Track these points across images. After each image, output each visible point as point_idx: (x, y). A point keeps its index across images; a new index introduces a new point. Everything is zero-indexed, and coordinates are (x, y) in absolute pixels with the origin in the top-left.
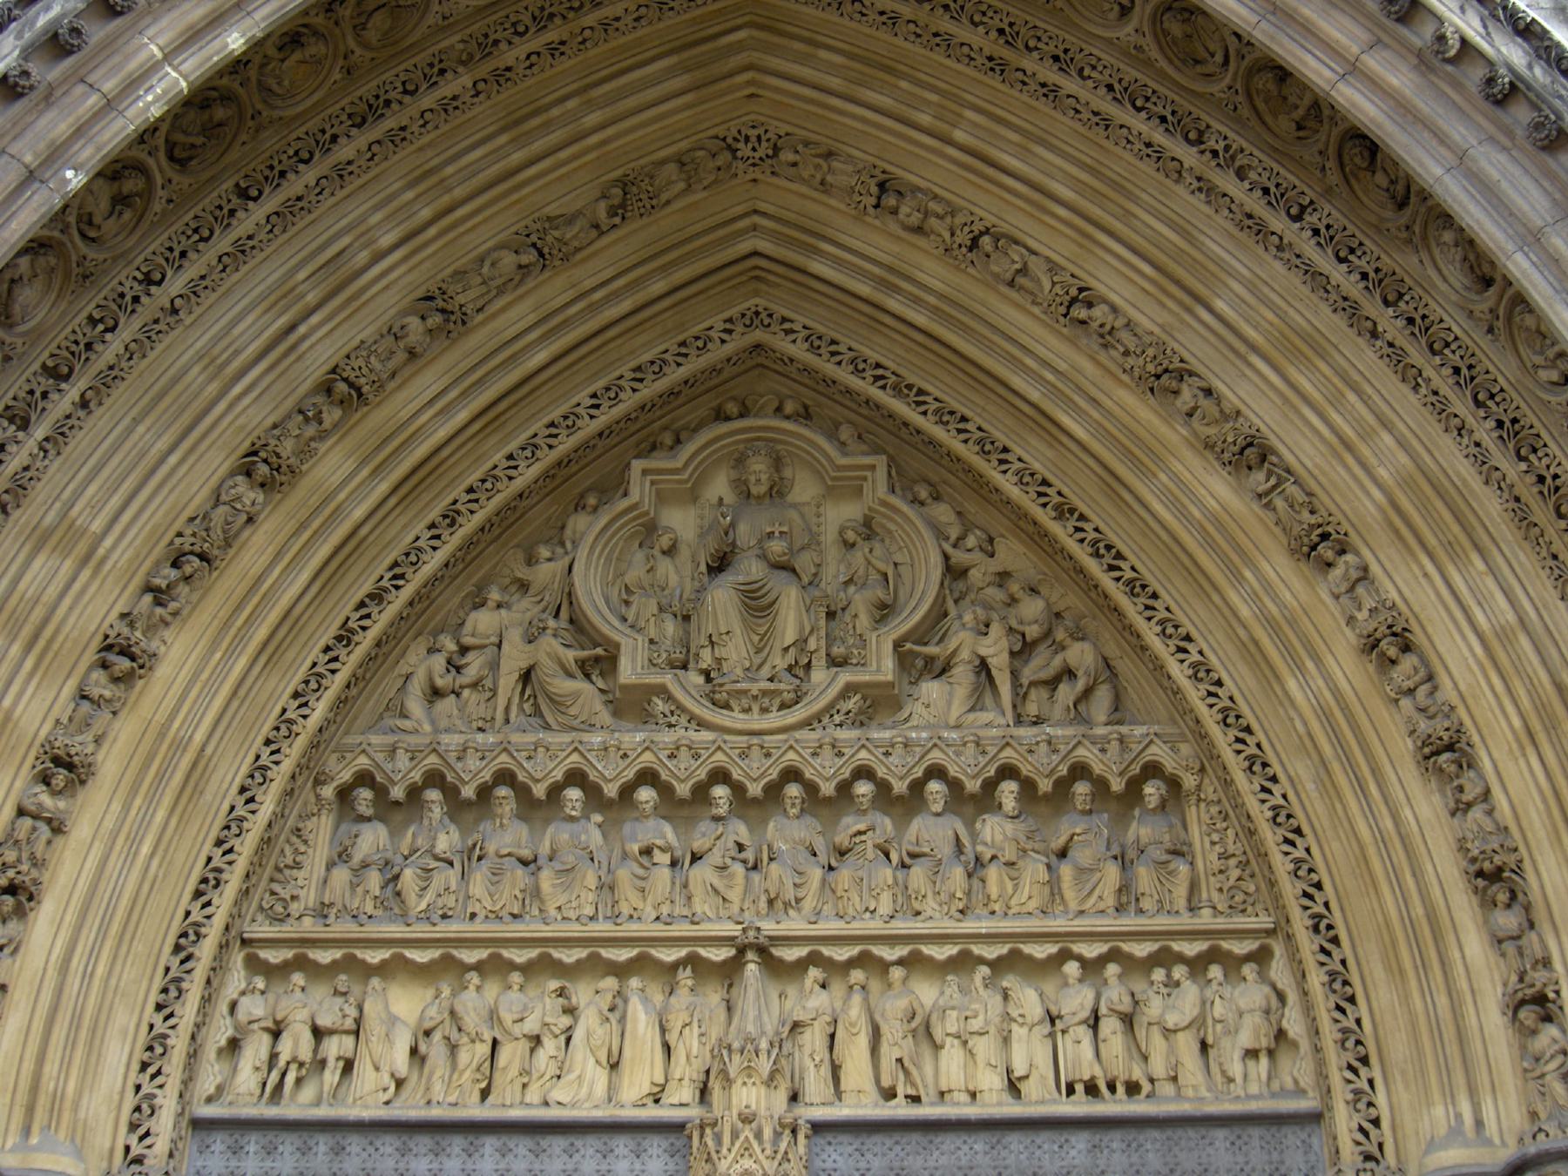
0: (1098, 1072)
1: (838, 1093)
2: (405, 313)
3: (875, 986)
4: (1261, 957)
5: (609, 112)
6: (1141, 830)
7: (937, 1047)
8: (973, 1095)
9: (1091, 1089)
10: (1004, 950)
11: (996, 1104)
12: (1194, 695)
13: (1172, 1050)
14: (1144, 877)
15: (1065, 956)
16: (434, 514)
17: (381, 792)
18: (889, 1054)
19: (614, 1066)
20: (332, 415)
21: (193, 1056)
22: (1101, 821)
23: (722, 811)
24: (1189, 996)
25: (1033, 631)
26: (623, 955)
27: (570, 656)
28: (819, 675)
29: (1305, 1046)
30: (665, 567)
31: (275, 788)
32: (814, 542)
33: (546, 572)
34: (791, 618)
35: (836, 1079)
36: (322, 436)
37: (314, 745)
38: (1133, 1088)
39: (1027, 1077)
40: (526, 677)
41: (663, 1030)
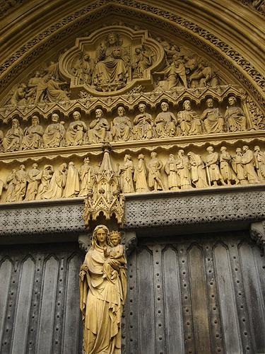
0: (221, 177)
3: (147, 159)
6: (229, 111)
7: (168, 175)
9: (219, 183)
14: (231, 122)
15: (208, 145)
19: (64, 188)
24: (249, 155)
25: (192, 67)
27: (57, 84)
30: (86, 63)
33: (53, 65)
35: (135, 186)
39: (197, 181)
40: (45, 92)
41: (79, 176)
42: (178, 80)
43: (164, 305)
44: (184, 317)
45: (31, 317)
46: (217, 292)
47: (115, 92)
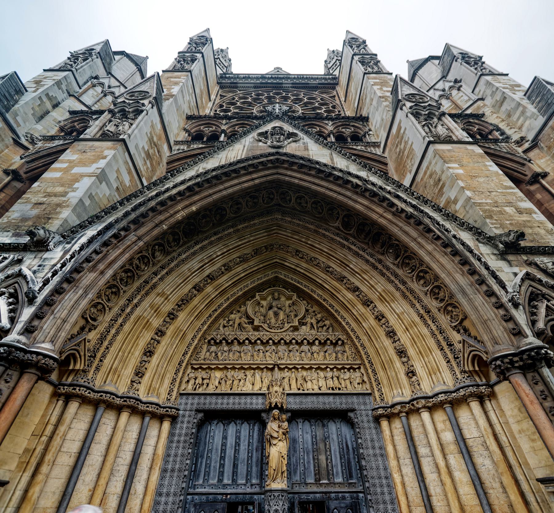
1: (291, 389)
2: (221, 266)
3: (296, 372)
4: (359, 368)
5: (254, 238)
6: (338, 348)
7: (306, 382)
8: (313, 390)
9: (333, 389)
10: (317, 366)
11: (317, 391)
12: (346, 327)
13: (345, 383)
14: (340, 355)
15: (327, 367)
16: (225, 298)
17: (215, 341)
18: (299, 383)
19: (253, 385)
20: (209, 281)
21: (181, 382)
22: (332, 347)
23: (271, 344)
26: (255, 366)
27: (246, 321)
28: (286, 325)
29: (367, 382)
30: (261, 309)
31: (197, 339)
32: (284, 306)
33: (243, 309)
34: (282, 316)
36: (208, 284)
37: (204, 333)
38: (339, 389)
40: (239, 324)
42: (312, 326)
43: (304, 452)
44: (314, 459)
45: (235, 456)
46: (330, 446)
47: (279, 331)
